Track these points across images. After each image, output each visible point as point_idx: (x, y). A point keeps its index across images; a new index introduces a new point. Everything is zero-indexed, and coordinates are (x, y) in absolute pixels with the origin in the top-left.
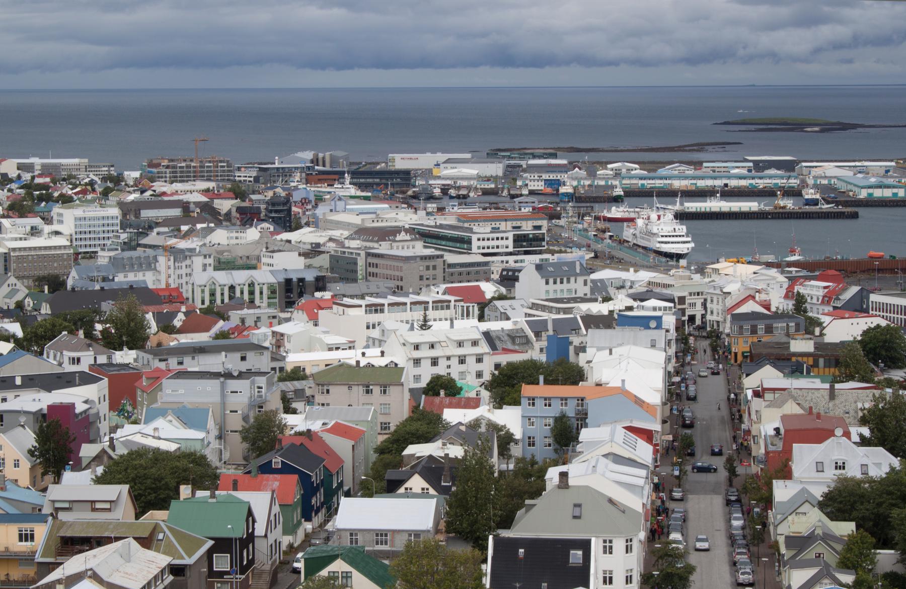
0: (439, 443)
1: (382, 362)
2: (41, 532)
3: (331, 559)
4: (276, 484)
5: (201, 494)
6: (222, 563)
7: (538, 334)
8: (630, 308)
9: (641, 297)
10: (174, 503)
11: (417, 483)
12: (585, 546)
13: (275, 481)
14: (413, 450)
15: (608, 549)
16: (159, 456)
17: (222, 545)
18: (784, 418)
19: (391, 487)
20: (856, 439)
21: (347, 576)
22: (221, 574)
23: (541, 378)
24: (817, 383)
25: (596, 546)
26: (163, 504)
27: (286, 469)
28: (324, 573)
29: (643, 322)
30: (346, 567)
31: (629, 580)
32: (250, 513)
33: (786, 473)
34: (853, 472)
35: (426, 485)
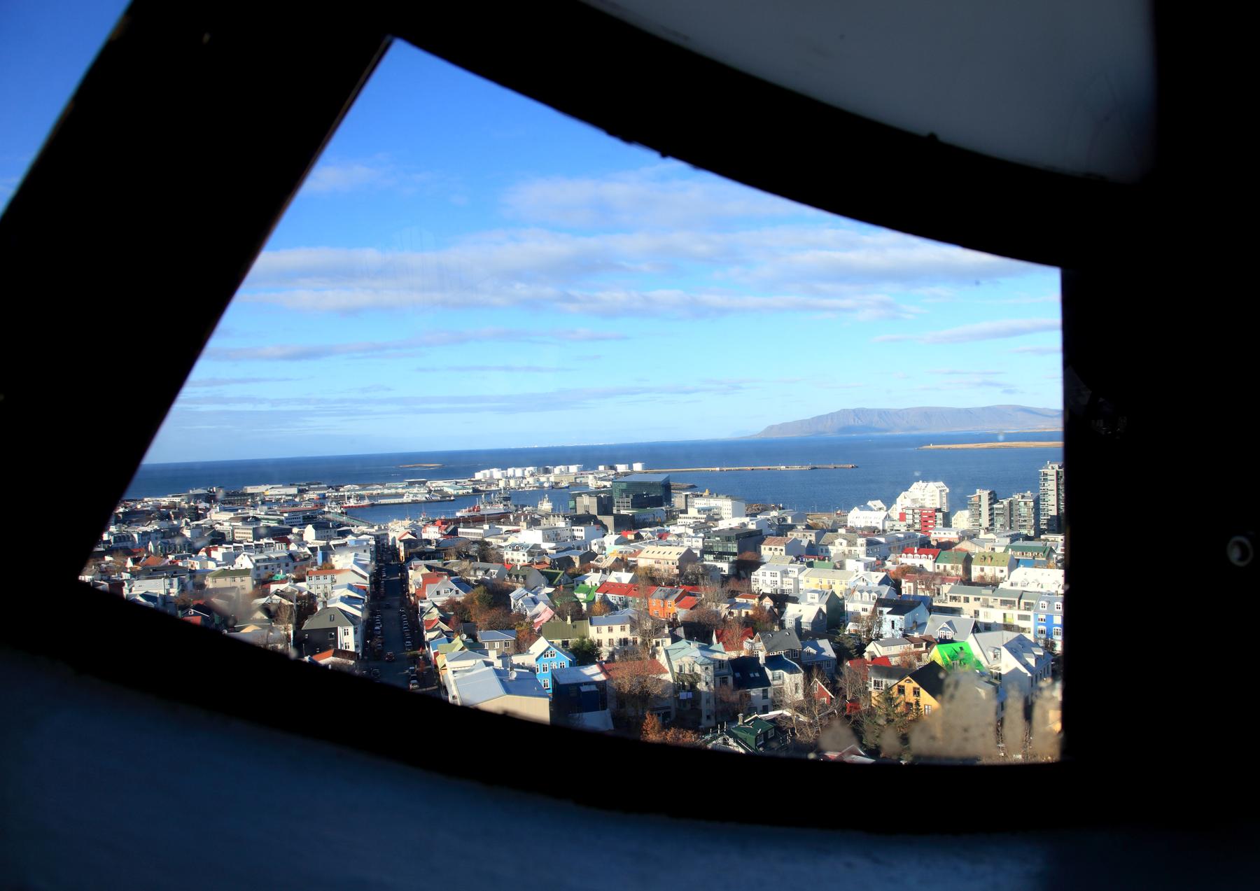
12: (335, 630)
25: (340, 630)
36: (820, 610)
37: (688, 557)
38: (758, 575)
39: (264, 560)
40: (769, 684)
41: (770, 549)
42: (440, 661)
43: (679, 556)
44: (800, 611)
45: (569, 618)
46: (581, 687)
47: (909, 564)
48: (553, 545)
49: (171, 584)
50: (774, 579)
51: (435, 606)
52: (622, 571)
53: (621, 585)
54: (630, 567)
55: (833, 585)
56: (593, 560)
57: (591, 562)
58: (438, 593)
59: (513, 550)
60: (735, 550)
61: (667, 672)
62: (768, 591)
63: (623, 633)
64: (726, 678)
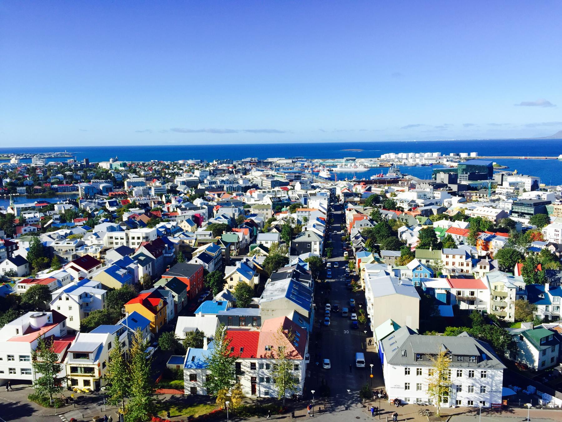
4: (244, 231)
5: (228, 233)
6: (233, 248)
9: (323, 189)
11: (274, 230)
12: (310, 243)
14: (274, 223)
15: (315, 244)
17: (233, 244)
21: (259, 250)
22: (232, 250)
25: (313, 243)
27: (246, 227)
28: (255, 250)
30: (259, 248)
31: (320, 251)
32: (238, 237)
35: (276, 230)
37: (503, 215)
40: (550, 304)
43: (496, 214)
45: (431, 248)
48: (423, 201)
49: (235, 211)
53: (461, 230)
54: (466, 218)
56: (445, 212)
57: (444, 213)
59: (401, 202)
60: (532, 212)
62: (553, 241)
63: (461, 259)
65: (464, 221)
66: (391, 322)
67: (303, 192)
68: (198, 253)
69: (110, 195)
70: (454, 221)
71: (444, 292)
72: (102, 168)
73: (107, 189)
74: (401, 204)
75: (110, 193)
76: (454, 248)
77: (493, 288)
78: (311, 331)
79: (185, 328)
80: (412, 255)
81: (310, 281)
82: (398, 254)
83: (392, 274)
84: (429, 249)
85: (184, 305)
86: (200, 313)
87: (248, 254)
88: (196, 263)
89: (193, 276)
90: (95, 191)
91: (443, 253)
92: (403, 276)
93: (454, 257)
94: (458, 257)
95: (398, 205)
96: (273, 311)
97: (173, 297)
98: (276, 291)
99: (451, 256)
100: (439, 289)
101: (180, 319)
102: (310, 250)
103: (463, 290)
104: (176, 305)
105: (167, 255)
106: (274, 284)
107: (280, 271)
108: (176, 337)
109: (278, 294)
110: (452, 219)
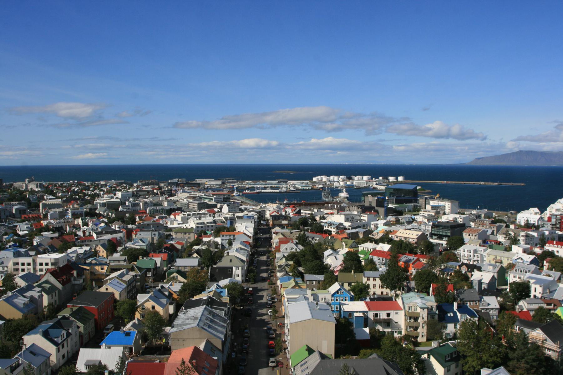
0: (200, 246)
1: (189, 227)
2: (106, 267)
3: (173, 273)
4: (163, 256)
5: (145, 258)
6: (149, 274)
7: (226, 220)
8: (247, 214)
9: (250, 211)
10: (138, 260)
11: (195, 255)
12: (232, 268)
13: (162, 255)
16: (136, 250)
17: (149, 270)
18: (279, 239)
19: (190, 256)
20: (295, 243)
21: (177, 276)
22: (149, 277)
23: (225, 230)
24: (287, 230)
25: (234, 269)
26: (136, 261)
27: (165, 252)
28: (172, 276)
29: (249, 217)
30: (177, 275)
31: (242, 276)
32: (156, 262)
33: (279, 251)
34: (294, 250)
35: (197, 255)
36: (493, 277)
37: (423, 237)
38: (461, 251)
39: (201, 223)
40: (458, 321)
41: (469, 235)
42: (283, 291)
43: (417, 237)
44: (482, 276)
46: (354, 314)
47: (550, 250)
48: (350, 224)
49: (155, 235)
50: (470, 254)
51: (284, 256)
52: (385, 243)
53: (383, 252)
54: (390, 241)
55: (503, 260)
56: (370, 234)
57: (370, 236)
58: (286, 249)
59: (329, 225)
60: (449, 234)
61: (401, 309)
62: (466, 262)
64: (435, 316)
65: (388, 244)
66: (306, 348)
67: (230, 215)
68: (109, 281)
69: (23, 218)
70: (378, 244)
71: (361, 314)
72: (16, 189)
73: (20, 211)
74: (330, 227)
75: (23, 216)
76: (375, 270)
77: (407, 309)
78: (225, 360)
79: (87, 361)
80: (331, 278)
81: (226, 309)
82: (321, 278)
83: (311, 299)
84: (351, 272)
85: (91, 336)
86: (104, 344)
87: (165, 281)
88: (107, 291)
89: (102, 304)
90: (7, 214)
91: (364, 276)
92: (322, 300)
93: (374, 280)
94: (378, 280)
95: (325, 229)
96: (184, 340)
97: (78, 327)
98: (188, 319)
99: (371, 279)
100: (357, 312)
101: (82, 350)
102: (230, 276)
103: (380, 312)
104: (81, 336)
105: (76, 282)
106: (186, 312)
107: (196, 298)
108: (77, 370)
109: (189, 322)
110: (377, 242)
